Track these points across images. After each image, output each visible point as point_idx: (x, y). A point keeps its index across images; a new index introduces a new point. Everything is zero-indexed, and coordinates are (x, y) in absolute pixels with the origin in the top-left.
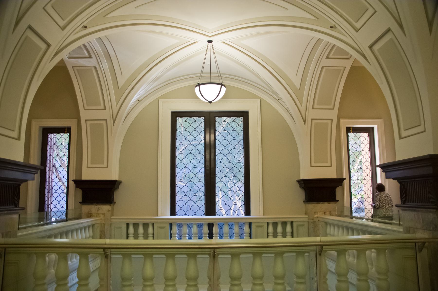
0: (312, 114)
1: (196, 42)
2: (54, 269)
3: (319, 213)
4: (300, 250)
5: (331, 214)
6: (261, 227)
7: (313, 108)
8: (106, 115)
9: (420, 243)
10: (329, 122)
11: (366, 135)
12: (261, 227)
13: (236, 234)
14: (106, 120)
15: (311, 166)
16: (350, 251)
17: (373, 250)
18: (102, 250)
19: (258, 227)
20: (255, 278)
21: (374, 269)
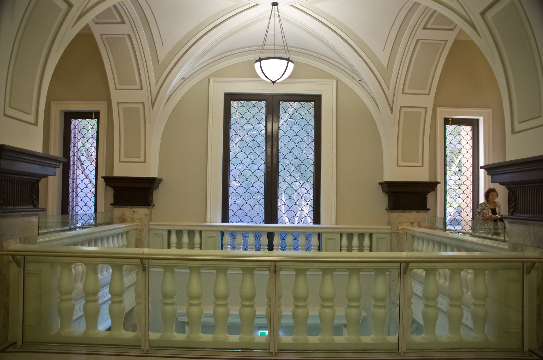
0: (401, 100)
1: (257, 5)
2: (81, 283)
4: (380, 267)
5: (419, 226)
6: (332, 239)
7: (403, 93)
8: (142, 96)
9: (529, 264)
10: (423, 110)
11: (468, 128)
13: (302, 246)
14: (143, 103)
15: (398, 166)
16: (441, 270)
17: (470, 271)
18: (139, 261)
19: (328, 238)
20: (324, 299)
21: (469, 293)
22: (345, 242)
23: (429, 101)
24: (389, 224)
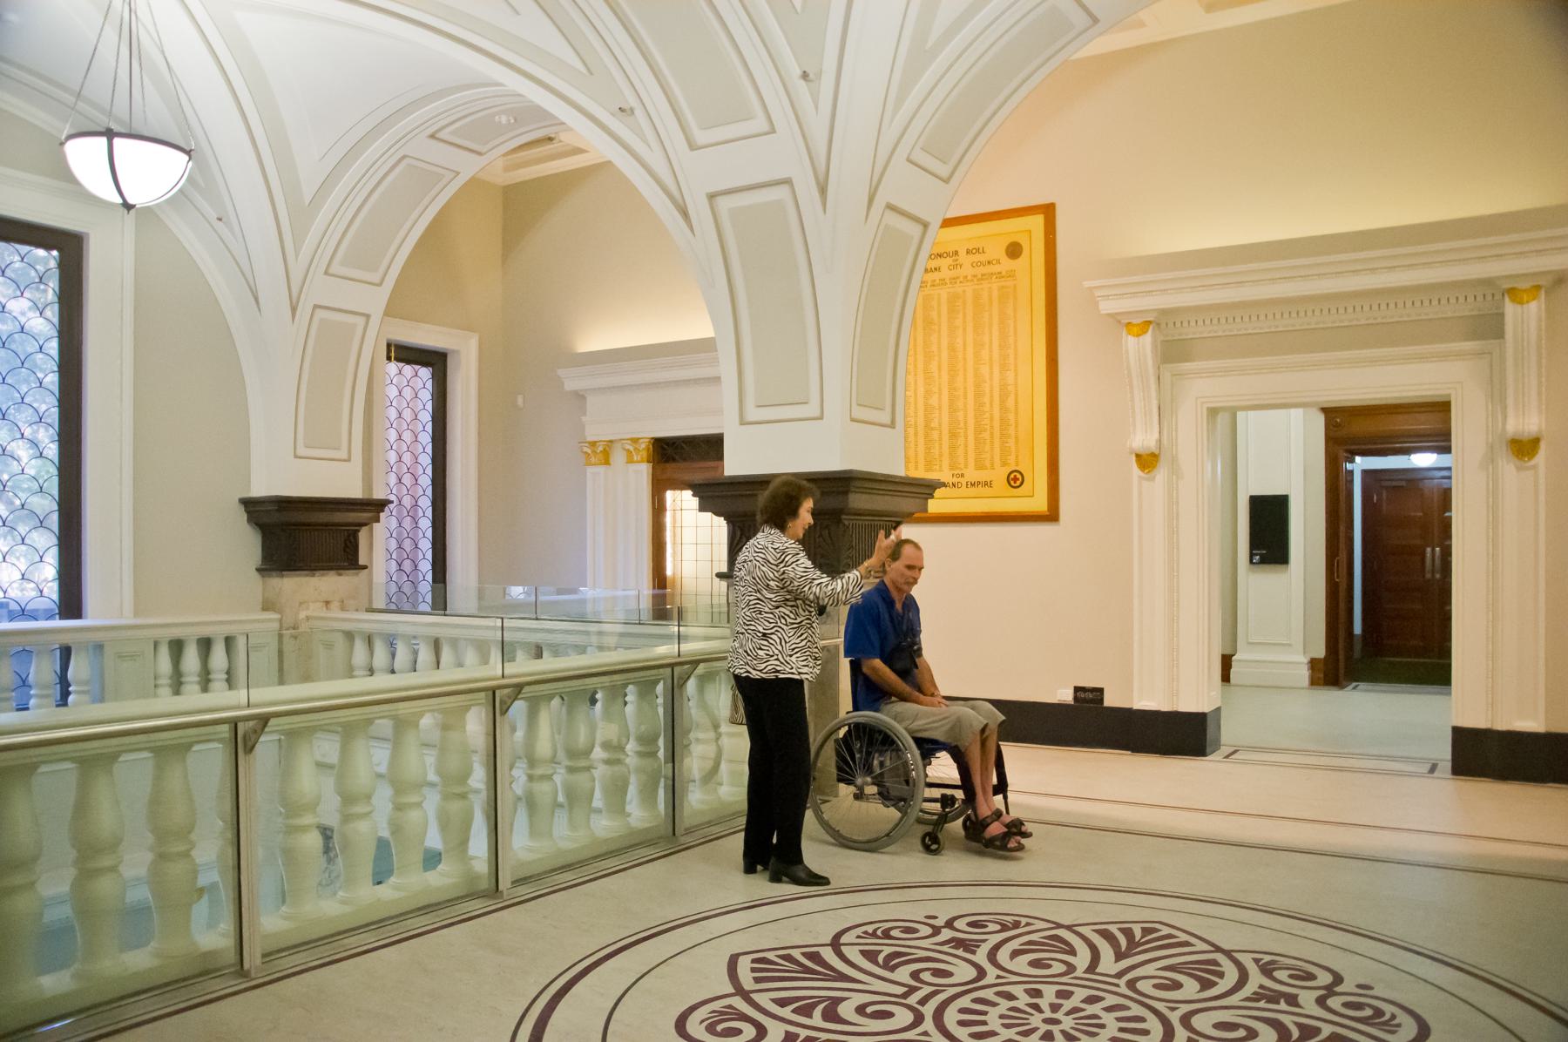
3: (312, 606)
5: (343, 609)
7: (326, 273)
10: (361, 321)
11: (425, 373)
19: (120, 656)
22: (165, 663)
23: (376, 301)
24: (267, 606)
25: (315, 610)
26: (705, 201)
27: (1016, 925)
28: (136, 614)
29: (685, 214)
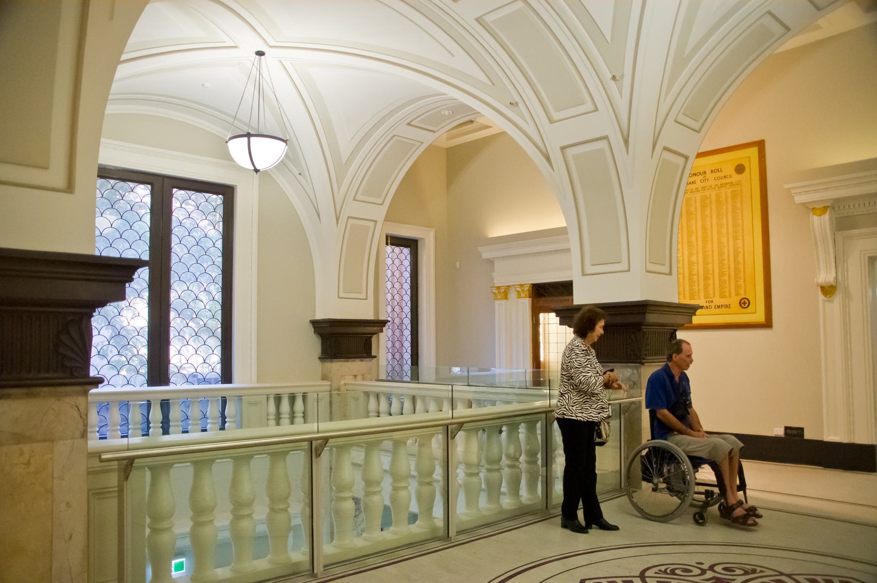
1: (236, 47)
5: (363, 379)
6: (256, 404)
7: (354, 199)
10: (373, 224)
11: (406, 251)
12: (256, 404)
13: (212, 419)
23: (379, 213)
24: (324, 378)
25: (349, 380)
26: (560, 151)
27: (754, 571)
28: (258, 382)
29: (548, 159)
